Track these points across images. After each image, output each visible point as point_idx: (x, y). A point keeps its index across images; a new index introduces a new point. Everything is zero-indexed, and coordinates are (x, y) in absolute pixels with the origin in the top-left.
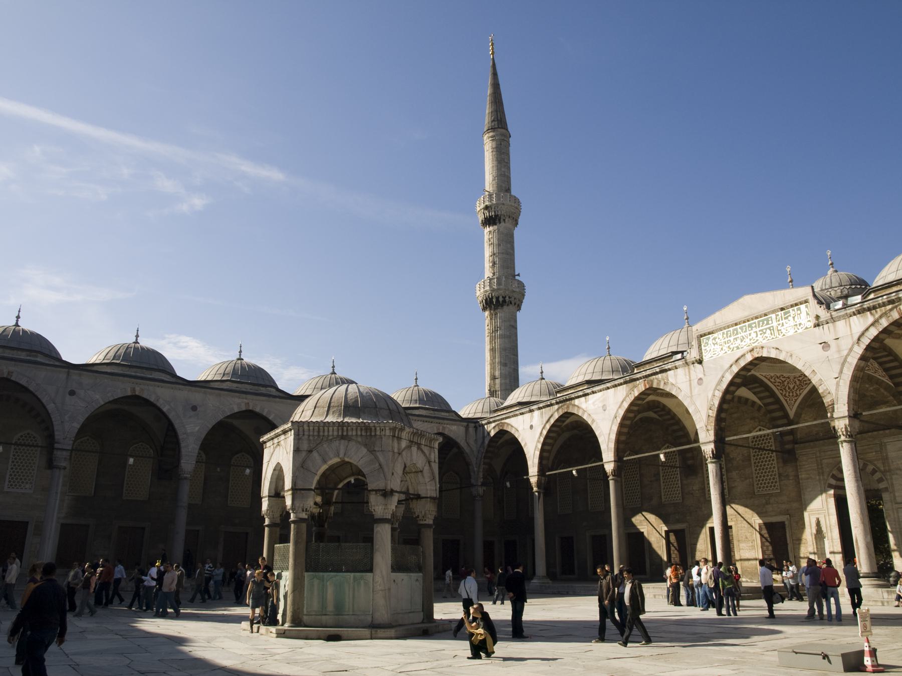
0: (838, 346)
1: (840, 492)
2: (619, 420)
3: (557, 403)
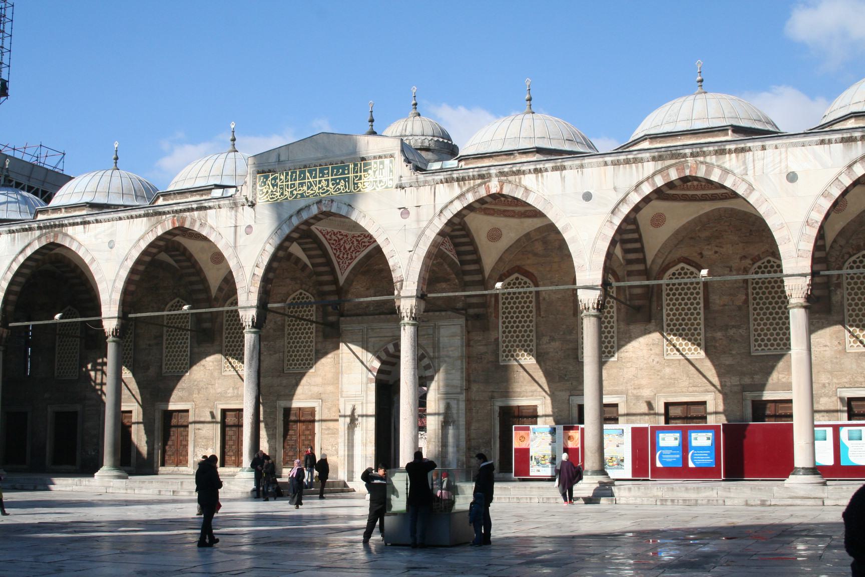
1: (390, 379)
2: (130, 264)
3: (40, 228)
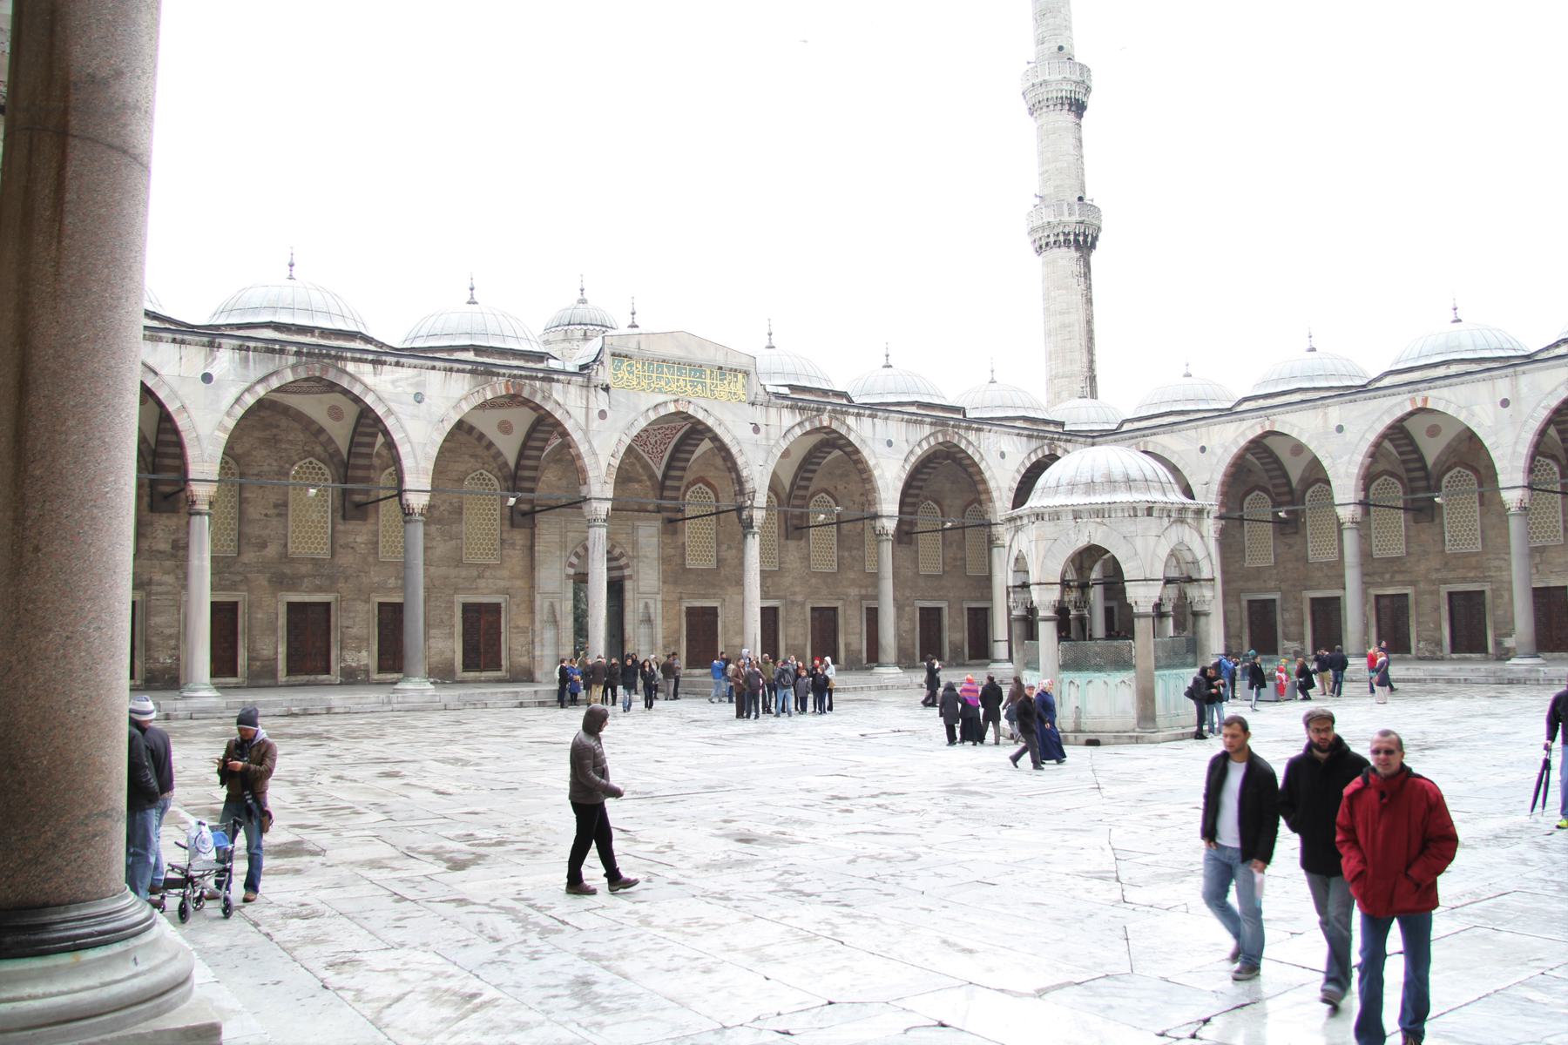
3: (298, 354)
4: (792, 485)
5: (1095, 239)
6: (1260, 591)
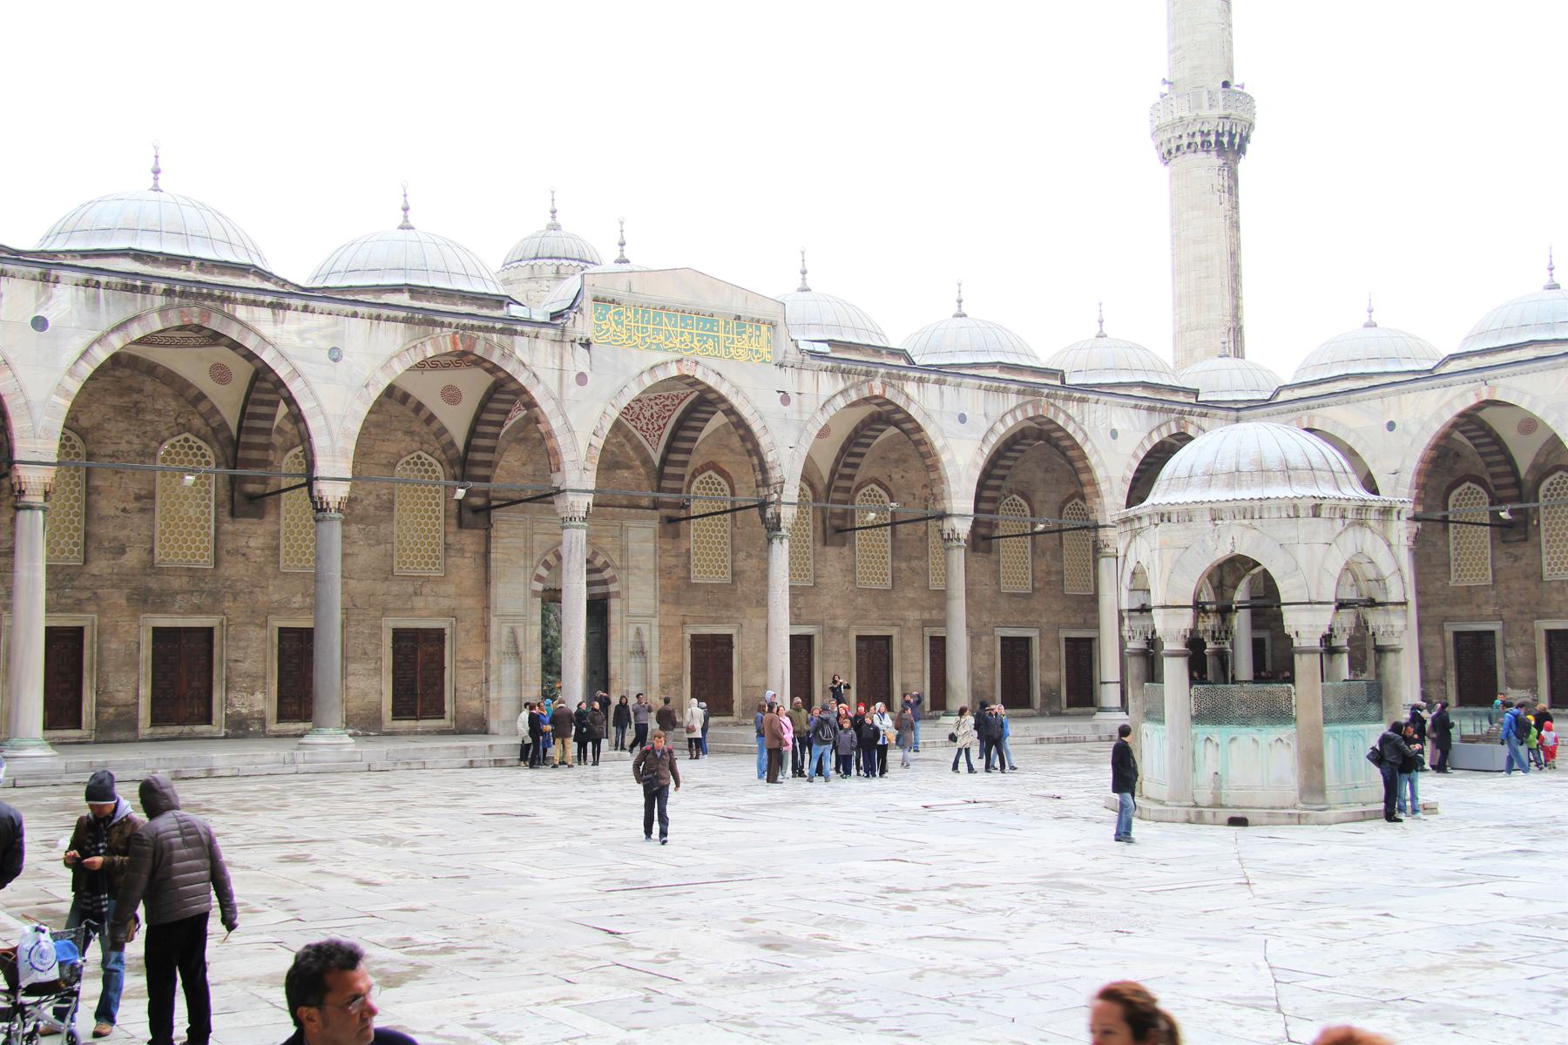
0: (800, 403)
3: (169, 293)
4: (833, 473)
5: (1245, 139)
6: (1471, 619)
